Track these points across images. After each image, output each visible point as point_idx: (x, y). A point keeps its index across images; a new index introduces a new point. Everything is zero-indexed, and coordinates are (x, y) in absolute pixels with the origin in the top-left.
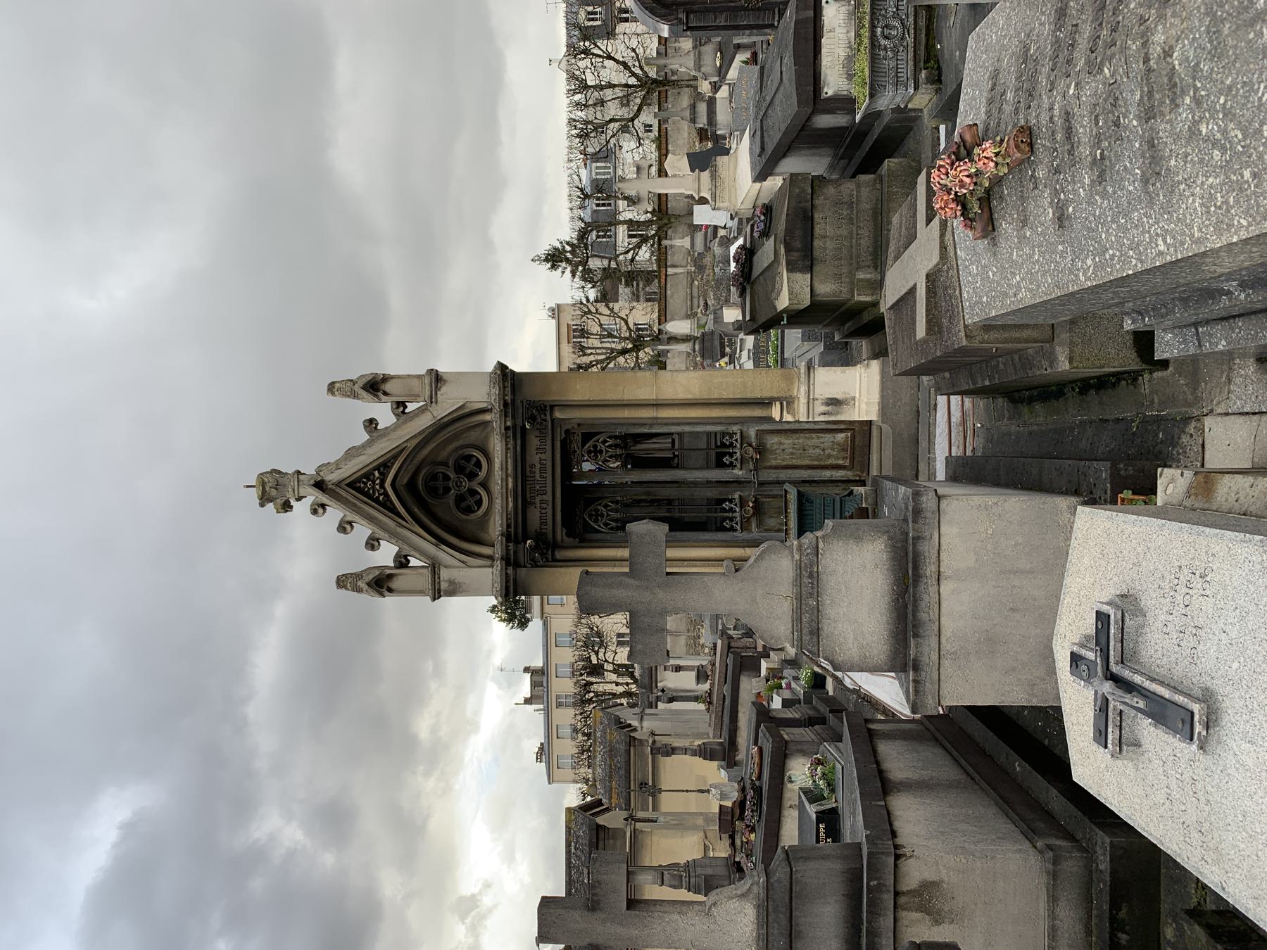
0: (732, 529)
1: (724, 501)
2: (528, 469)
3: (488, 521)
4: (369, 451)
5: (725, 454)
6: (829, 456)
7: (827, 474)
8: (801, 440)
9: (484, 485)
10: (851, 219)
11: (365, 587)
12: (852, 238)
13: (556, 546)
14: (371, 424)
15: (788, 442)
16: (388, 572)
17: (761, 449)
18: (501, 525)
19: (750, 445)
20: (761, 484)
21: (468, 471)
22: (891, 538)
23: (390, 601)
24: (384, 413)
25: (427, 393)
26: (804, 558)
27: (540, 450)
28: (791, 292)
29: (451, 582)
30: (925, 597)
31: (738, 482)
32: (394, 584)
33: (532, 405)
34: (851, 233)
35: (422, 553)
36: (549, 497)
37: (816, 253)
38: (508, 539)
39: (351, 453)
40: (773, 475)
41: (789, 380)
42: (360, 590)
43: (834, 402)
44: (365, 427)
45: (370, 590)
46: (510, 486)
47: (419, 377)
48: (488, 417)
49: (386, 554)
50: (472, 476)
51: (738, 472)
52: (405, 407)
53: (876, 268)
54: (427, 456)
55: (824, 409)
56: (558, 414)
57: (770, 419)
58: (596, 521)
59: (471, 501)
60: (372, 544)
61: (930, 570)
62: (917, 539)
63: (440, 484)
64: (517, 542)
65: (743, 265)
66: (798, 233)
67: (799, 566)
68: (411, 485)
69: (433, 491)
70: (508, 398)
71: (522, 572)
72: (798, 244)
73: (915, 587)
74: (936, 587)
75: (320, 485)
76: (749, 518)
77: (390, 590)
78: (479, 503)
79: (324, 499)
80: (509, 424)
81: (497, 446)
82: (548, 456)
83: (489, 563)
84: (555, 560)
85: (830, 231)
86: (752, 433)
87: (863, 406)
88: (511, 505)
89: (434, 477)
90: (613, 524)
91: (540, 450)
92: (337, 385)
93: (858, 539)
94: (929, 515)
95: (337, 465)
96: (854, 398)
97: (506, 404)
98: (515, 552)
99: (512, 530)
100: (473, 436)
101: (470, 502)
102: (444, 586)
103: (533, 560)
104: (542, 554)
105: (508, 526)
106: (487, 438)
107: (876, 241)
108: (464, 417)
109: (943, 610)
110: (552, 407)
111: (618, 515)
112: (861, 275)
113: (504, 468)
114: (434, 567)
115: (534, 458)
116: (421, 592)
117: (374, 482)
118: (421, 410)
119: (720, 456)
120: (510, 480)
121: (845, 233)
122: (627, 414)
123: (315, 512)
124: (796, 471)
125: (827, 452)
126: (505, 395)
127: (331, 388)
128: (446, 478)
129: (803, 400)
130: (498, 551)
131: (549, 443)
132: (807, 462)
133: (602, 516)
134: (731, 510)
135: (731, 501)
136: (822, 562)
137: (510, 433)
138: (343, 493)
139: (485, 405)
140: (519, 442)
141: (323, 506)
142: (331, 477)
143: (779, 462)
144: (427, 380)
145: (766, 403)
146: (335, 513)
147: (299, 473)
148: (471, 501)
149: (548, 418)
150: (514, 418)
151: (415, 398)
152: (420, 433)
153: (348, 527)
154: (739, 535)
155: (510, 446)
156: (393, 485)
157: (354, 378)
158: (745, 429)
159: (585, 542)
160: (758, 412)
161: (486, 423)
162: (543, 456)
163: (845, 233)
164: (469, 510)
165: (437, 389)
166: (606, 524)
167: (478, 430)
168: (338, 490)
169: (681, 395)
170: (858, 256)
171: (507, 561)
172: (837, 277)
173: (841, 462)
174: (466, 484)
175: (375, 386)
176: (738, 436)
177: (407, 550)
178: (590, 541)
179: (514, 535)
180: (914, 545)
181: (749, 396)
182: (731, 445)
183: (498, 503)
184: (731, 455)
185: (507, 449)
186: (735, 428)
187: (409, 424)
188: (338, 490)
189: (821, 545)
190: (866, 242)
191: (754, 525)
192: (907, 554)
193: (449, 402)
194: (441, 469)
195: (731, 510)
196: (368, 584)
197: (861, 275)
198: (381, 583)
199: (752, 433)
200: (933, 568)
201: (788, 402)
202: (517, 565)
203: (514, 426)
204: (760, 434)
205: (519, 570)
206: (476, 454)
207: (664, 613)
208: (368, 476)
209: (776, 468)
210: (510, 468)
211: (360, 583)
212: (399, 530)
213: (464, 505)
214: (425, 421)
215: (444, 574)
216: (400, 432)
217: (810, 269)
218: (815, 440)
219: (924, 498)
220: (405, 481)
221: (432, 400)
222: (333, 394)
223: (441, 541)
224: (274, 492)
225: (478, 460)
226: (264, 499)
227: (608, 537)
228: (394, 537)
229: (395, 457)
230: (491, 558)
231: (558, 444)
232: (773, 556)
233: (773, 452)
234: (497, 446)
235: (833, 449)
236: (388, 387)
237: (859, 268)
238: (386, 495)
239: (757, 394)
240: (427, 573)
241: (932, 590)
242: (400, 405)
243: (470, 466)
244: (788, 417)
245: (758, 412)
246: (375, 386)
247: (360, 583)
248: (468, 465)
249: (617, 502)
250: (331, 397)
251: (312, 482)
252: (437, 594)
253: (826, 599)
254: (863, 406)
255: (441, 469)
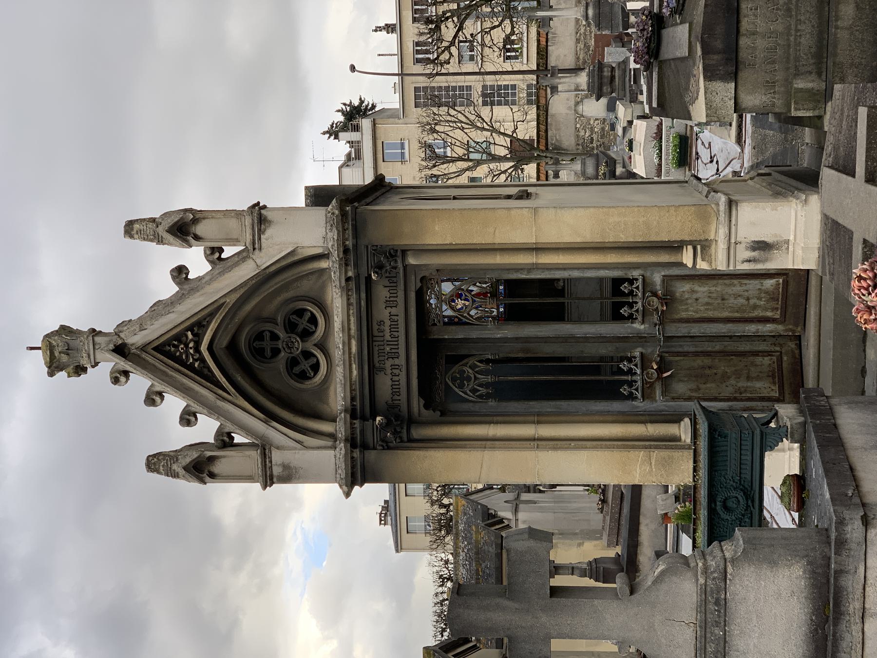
0: (631, 397)
1: (622, 359)
2: (375, 327)
3: (328, 388)
4: (180, 308)
5: (623, 304)
6: (755, 307)
7: (751, 328)
8: (718, 287)
9: (322, 346)
10: (789, 10)
11: (182, 472)
12: (789, 34)
13: (412, 421)
14: (180, 273)
15: (702, 289)
16: (209, 454)
17: (668, 299)
18: (344, 399)
19: (655, 294)
20: (668, 339)
21: (300, 328)
22: (810, 563)
23: (213, 488)
24: (195, 260)
25: (249, 237)
26: (709, 582)
27: (390, 303)
28: (709, 106)
29: (286, 467)
30: (847, 637)
31: (641, 339)
32: (217, 468)
33: (378, 250)
34: (788, 28)
35: (246, 430)
36: (402, 361)
37: (743, 54)
38: (353, 416)
39: (160, 308)
40: (683, 330)
41: (703, 215)
42: (176, 475)
43: (762, 246)
44: (174, 278)
45: (187, 475)
46: (354, 349)
47: (238, 214)
48: (324, 264)
49: (206, 429)
50: (306, 334)
51: (638, 326)
52: (221, 250)
53: (819, 74)
54: (250, 313)
55: (749, 254)
56: (412, 261)
57: (681, 265)
58: (461, 387)
59: (305, 365)
60: (188, 418)
61: (854, 606)
62: (839, 573)
63: (267, 344)
64: (364, 418)
65: (649, 40)
66: (720, 29)
67: (704, 591)
68: (232, 347)
69: (259, 353)
70: (349, 243)
71: (371, 455)
72: (719, 44)
73: (836, 625)
74: (860, 625)
75: (121, 350)
76: (652, 385)
77: (212, 476)
78: (316, 367)
79: (126, 365)
80: (350, 274)
81: (336, 301)
82: (400, 310)
83: (330, 443)
84: (411, 440)
85: (761, 25)
86: (657, 278)
87: (799, 252)
88: (355, 373)
89: (260, 336)
90: (483, 391)
91: (390, 303)
92: (136, 226)
93: (773, 564)
94: (853, 546)
95: (141, 323)
96: (787, 242)
97: (346, 251)
98: (362, 432)
99: (358, 403)
100: (306, 287)
101: (303, 367)
102: (277, 470)
103: (384, 440)
104: (395, 433)
105: (353, 399)
106: (323, 288)
107: (821, 33)
108: (294, 264)
109: (867, 650)
110: (404, 252)
111: (489, 379)
112: (800, 84)
113: (346, 329)
114: (264, 448)
115: (382, 313)
116: (250, 478)
117: (187, 345)
118: (241, 257)
119: (617, 306)
120: (354, 343)
121: (780, 28)
122: (499, 259)
123: (116, 381)
124: (712, 325)
125: (752, 302)
126: (345, 239)
127: (130, 228)
128: (274, 337)
129: (722, 246)
130: (340, 428)
131: (401, 294)
132: (726, 314)
133: (469, 379)
134: (630, 372)
135: (630, 360)
136: (731, 588)
137: (352, 285)
138: (149, 359)
139: (319, 251)
140: (363, 295)
141: (126, 374)
142: (136, 339)
143: (691, 314)
144: (248, 221)
145: (676, 247)
146: (140, 383)
147: (94, 330)
148: (305, 365)
149: (400, 265)
150: (356, 266)
151: (234, 242)
152: (241, 286)
153: (158, 399)
154: (640, 404)
155: (353, 300)
156: (210, 348)
157: (157, 215)
158: (648, 274)
159: (447, 416)
160: (664, 258)
161: (322, 271)
162: (394, 311)
163: (780, 28)
164: (303, 376)
165: (261, 232)
166: (474, 391)
167: (314, 277)
168: (144, 355)
169: (568, 238)
170: (797, 59)
171: (352, 442)
172: (770, 85)
173: (769, 314)
174: (299, 346)
175: (183, 228)
176: (640, 283)
177: (229, 427)
178: (455, 413)
179: (361, 409)
180: (836, 579)
181: (654, 238)
182: (631, 293)
183: (339, 372)
184: (631, 305)
185: (349, 304)
186: (636, 273)
187: (227, 275)
188: (144, 355)
189: (730, 569)
190: (807, 41)
191: (658, 392)
192: (828, 581)
193: (276, 246)
194: (269, 327)
195: (630, 372)
196: (185, 468)
197: (800, 84)
198: (201, 466)
199: (657, 278)
200: (857, 605)
201: (703, 246)
202: (365, 447)
203: (358, 276)
204: (667, 279)
205: (367, 453)
206: (310, 307)
207: (547, 639)
208: (179, 338)
209: (688, 321)
210: (353, 327)
211: (175, 467)
212: (220, 403)
213: (297, 370)
214: (246, 272)
215: (277, 457)
216: (216, 285)
217: (734, 76)
218: (737, 287)
219: (849, 528)
220: (225, 343)
221: (255, 245)
222: (132, 237)
223: (270, 417)
224: (64, 358)
225: (313, 314)
226: (54, 367)
227: (477, 407)
228: (213, 411)
229: (212, 315)
230: (332, 436)
231: (412, 296)
232: (674, 579)
233: (683, 302)
234: (336, 301)
235: (760, 299)
236: (200, 229)
237: (797, 74)
238: (202, 360)
239: (664, 237)
240: (255, 455)
241: (856, 629)
242: (214, 253)
243: (303, 323)
244: (702, 265)
245: (664, 258)
246: (183, 228)
247: (175, 467)
248: (303, 321)
249: (488, 361)
250: (128, 240)
251: (111, 346)
252: (268, 480)
253: (734, 629)
254: (799, 252)
255: (269, 327)
